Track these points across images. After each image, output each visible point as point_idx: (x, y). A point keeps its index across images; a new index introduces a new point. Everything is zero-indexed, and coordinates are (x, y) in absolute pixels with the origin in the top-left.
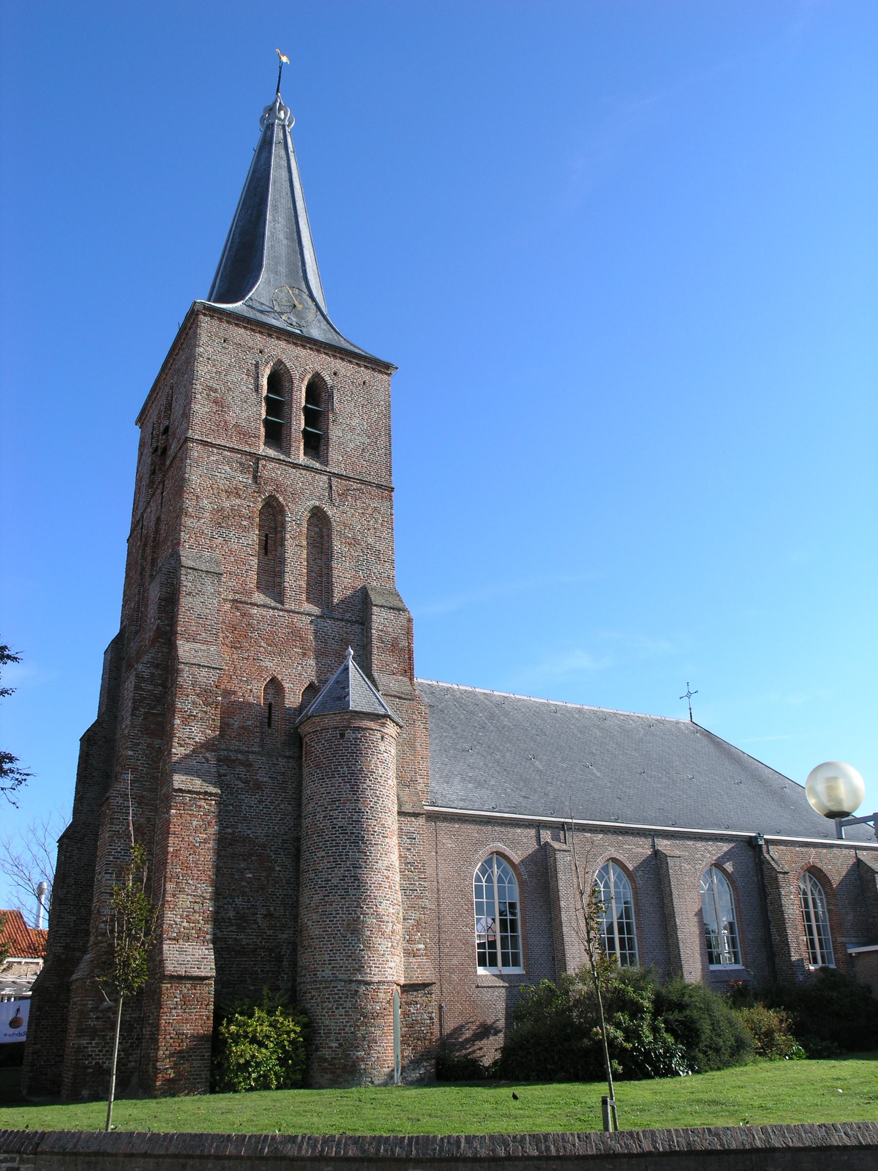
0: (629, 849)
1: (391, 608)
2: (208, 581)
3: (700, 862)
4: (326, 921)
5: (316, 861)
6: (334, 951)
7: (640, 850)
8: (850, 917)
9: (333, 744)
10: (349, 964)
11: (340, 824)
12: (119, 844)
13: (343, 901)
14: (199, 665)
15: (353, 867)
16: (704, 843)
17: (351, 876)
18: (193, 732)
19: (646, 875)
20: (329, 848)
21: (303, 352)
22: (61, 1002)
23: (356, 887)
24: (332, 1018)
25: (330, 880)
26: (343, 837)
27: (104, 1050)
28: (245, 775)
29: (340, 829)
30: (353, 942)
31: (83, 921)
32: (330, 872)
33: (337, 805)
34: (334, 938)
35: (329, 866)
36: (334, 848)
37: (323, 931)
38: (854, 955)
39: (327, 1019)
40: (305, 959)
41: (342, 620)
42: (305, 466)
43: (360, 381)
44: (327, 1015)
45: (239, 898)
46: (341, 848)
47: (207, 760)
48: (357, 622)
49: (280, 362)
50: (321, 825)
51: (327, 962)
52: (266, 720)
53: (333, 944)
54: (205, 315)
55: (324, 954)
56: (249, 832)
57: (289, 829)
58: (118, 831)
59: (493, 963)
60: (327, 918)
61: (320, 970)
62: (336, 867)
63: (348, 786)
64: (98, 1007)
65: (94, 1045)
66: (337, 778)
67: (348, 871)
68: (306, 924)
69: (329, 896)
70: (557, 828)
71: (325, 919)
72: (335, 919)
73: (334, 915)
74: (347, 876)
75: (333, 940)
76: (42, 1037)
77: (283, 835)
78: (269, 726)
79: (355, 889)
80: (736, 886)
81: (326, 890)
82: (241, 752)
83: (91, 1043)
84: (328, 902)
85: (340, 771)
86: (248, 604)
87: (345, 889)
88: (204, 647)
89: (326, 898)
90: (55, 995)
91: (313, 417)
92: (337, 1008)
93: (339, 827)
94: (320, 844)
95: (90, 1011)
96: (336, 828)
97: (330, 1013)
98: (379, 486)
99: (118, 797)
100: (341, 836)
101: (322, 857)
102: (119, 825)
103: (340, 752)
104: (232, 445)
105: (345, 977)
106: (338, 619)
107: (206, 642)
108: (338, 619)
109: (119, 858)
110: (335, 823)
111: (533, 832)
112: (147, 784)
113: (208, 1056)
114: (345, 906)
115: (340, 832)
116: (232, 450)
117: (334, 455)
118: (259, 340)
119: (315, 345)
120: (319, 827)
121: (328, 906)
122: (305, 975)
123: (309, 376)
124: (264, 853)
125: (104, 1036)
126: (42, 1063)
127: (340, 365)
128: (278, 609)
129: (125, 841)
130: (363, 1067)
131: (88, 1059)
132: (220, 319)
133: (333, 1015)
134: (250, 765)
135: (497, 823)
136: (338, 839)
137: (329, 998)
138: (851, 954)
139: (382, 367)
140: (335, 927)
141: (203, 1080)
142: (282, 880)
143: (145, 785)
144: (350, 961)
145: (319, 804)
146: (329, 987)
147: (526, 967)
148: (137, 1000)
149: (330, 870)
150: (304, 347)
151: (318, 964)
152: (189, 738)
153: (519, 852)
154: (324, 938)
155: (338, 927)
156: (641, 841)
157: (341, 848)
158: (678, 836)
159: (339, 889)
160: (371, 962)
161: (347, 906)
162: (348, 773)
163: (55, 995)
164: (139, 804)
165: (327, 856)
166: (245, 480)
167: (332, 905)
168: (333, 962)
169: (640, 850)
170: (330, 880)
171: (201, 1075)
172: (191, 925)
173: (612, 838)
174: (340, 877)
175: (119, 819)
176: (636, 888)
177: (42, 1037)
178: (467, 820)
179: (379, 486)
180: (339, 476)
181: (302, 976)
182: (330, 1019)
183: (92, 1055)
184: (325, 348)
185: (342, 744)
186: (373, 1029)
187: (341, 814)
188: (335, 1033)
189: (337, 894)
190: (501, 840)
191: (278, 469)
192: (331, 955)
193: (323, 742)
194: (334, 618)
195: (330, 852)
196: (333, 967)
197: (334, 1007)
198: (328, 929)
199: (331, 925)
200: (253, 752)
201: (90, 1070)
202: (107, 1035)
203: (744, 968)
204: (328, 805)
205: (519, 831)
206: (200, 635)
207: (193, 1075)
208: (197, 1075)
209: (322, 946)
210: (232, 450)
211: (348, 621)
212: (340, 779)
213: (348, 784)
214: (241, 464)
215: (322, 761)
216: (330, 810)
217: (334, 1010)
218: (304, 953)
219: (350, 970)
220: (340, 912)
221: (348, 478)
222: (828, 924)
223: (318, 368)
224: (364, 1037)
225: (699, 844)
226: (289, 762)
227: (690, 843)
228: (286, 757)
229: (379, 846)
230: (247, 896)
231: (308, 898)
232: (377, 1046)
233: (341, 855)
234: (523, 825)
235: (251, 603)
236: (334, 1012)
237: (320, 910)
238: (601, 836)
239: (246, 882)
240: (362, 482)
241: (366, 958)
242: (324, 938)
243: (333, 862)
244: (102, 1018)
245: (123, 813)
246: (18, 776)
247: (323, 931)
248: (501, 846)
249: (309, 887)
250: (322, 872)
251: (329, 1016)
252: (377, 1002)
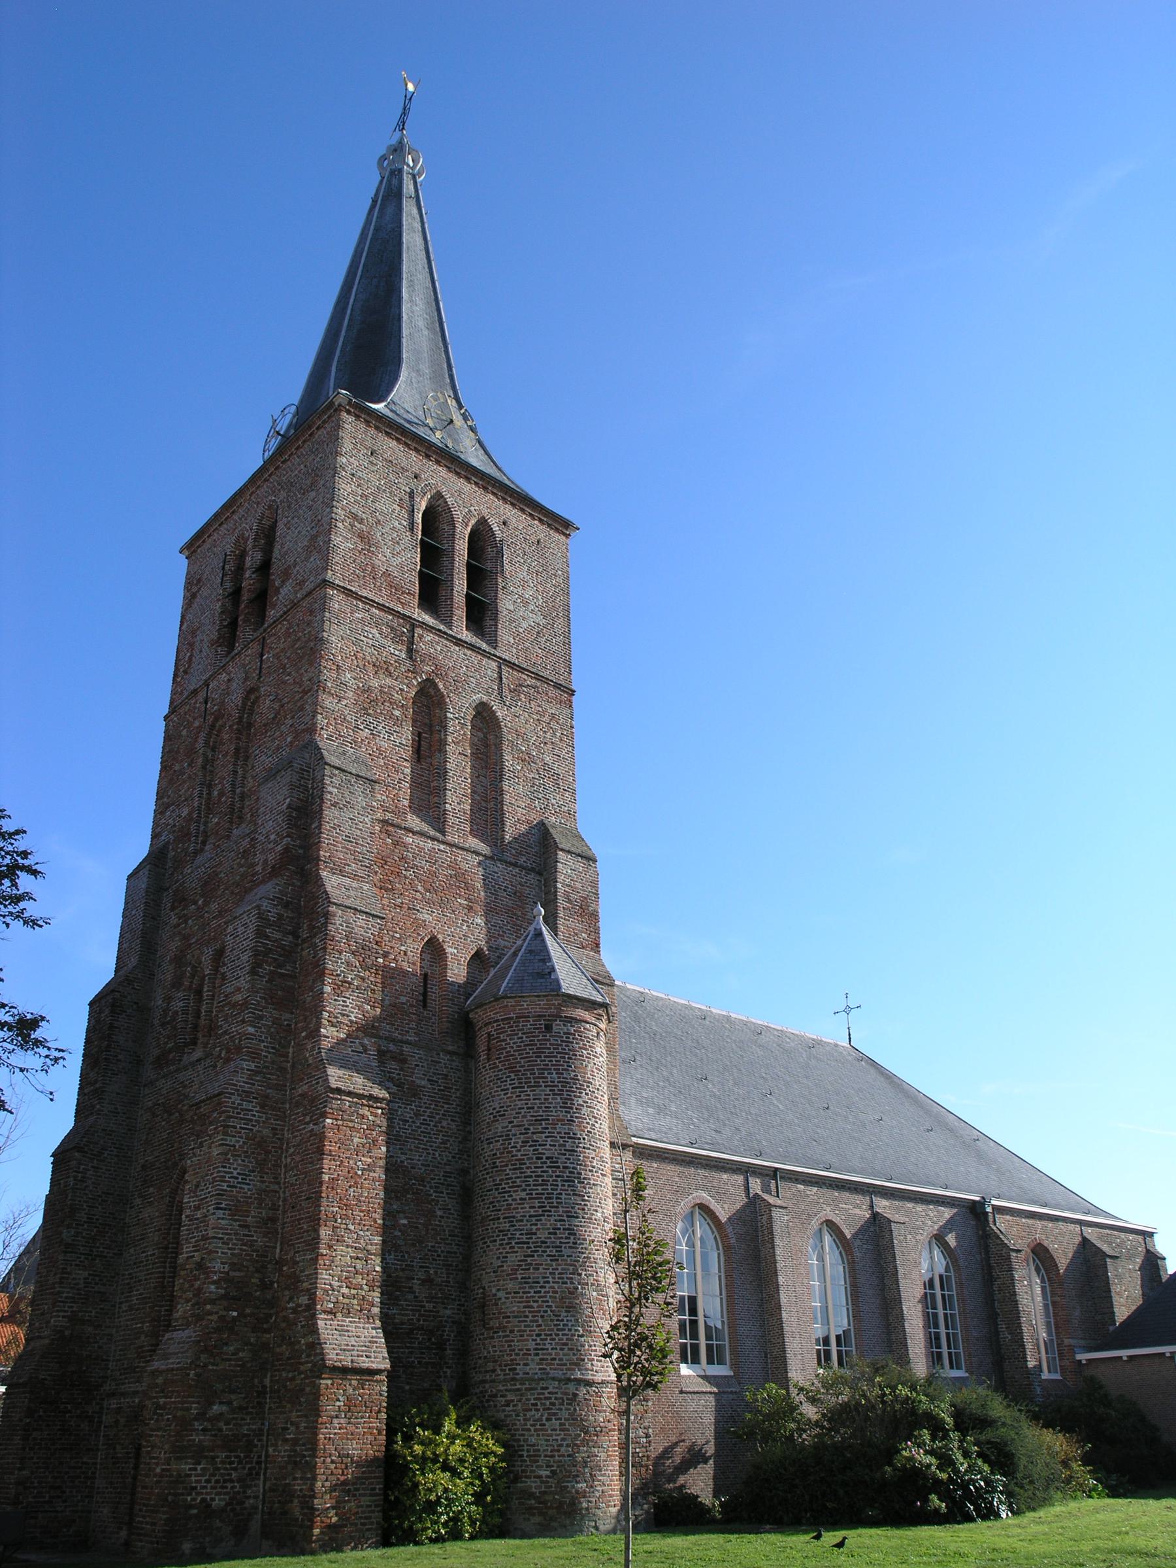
0: (846, 1210)
1: (579, 855)
2: (358, 788)
3: (921, 1231)
4: (529, 1293)
5: (511, 1205)
6: (543, 1337)
7: (857, 1211)
8: (1077, 1313)
10: (564, 1355)
11: (548, 1154)
12: (235, 1166)
13: (554, 1263)
14: (356, 909)
15: (568, 1216)
16: (924, 1207)
17: (564, 1229)
18: (347, 1006)
19: (865, 1246)
20: (532, 1187)
21: (468, 488)
22: (64, 1403)
23: (571, 1245)
24: (541, 1433)
25: (535, 1234)
26: (553, 1172)
27: (213, 1479)
28: (399, 1074)
30: (570, 1324)
31: (97, 1279)
32: (534, 1222)
33: (544, 1126)
34: (542, 1317)
35: (532, 1213)
36: (540, 1188)
37: (524, 1307)
38: (1084, 1362)
39: (533, 1435)
40: (495, 1346)
41: (515, 865)
43: (534, 539)
44: (532, 1429)
45: (390, 1255)
46: (549, 1187)
47: (366, 1050)
48: (533, 870)
49: (439, 496)
50: (519, 1154)
51: (532, 1352)
52: (421, 998)
53: (540, 1326)
54: (349, 412)
55: (528, 1340)
56: (404, 1157)
57: (454, 1157)
58: (234, 1146)
59: (696, 1360)
60: (531, 1287)
61: (521, 1363)
62: (544, 1215)
63: (559, 1100)
64: (204, 1414)
65: (199, 1471)
66: (543, 1088)
67: (560, 1221)
68: (495, 1295)
69: (533, 1256)
70: (767, 1175)
71: (527, 1290)
72: (543, 1290)
73: (542, 1284)
74: (559, 1229)
75: (540, 1320)
76: (32, 1458)
77: (445, 1164)
78: (425, 1006)
79: (570, 1247)
80: (959, 1266)
81: (528, 1248)
82: (394, 1041)
83: (195, 1469)
84: (531, 1264)
85: (547, 1078)
86: (401, 828)
87: (557, 1247)
88: (355, 884)
89: (529, 1259)
90: (53, 1392)
92: (548, 1420)
93: (547, 1158)
94: (518, 1180)
95: (196, 1419)
96: (542, 1158)
97: (538, 1427)
98: (558, 686)
99: (233, 1094)
100: (550, 1170)
101: (521, 1199)
102: (235, 1136)
104: (381, 602)
105: (559, 1374)
106: (511, 864)
107: (355, 877)
108: (511, 864)
109: (236, 1187)
110: (540, 1151)
111: (740, 1179)
112: (272, 1077)
113: (380, 1489)
114: (557, 1272)
115: (549, 1164)
116: (382, 607)
117: (505, 635)
118: (413, 460)
119: (482, 479)
120: (516, 1156)
121: (531, 1271)
122: (494, 1371)
123: (473, 522)
124: (422, 1190)
125: (213, 1458)
126: (31, 1500)
128: (438, 841)
129: (243, 1161)
130: (585, 1505)
131: (190, 1494)
132: (367, 423)
133: (542, 1430)
134: (404, 1061)
135: (701, 1164)
136: (545, 1174)
137: (536, 1404)
138: (1080, 1361)
140: (543, 1301)
141: (374, 1527)
142: (444, 1231)
143: (270, 1079)
144: (566, 1351)
145: (515, 1123)
146: (536, 1389)
147: (734, 1366)
148: (258, 1403)
149: (534, 1219)
150: (468, 479)
151: (518, 1355)
152: (343, 1015)
153: (726, 1206)
154: (527, 1317)
155: (548, 1302)
156: (859, 1199)
157: (549, 1187)
158: (897, 1196)
159: (548, 1247)
160: (593, 1353)
161: (560, 1271)
162: (558, 1082)
163: (53, 1392)
164: (262, 1107)
165: (530, 1199)
166: (397, 653)
167: (538, 1269)
168: (540, 1352)
169: (857, 1211)
170: (535, 1234)
171: (370, 1518)
172: (353, 1292)
173: (827, 1192)
174: (549, 1229)
175: (235, 1127)
176: (854, 1262)
177: (32, 1458)
178: (666, 1158)
179: (558, 686)
180: (512, 665)
181: (487, 1372)
182: (538, 1435)
183: (196, 1487)
184: (494, 486)
185: (549, 1040)
186: (596, 1450)
187: (549, 1139)
188: (546, 1456)
189: (545, 1255)
191: (438, 643)
192: (538, 1342)
193: (520, 1035)
194: (506, 862)
195: (534, 1192)
196: (541, 1359)
197: (544, 1418)
198: (532, 1303)
199: (537, 1298)
200: (408, 1043)
201: (195, 1511)
202: (218, 1457)
203: (967, 1375)
204: (530, 1125)
205: (725, 1176)
206: (349, 865)
207: (361, 1518)
208: (366, 1518)
209: (523, 1328)
210: (382, 607)
211: (522, 867)
212: (548, 1089)
213: (558, 1097)
214: (392, 629)
215: (520, 1062)
216: (533, 1133)
217: (544, 1422)
218: (493, 1338)
219: (566, 1365)
220: (550, 1279)
221: (522, 670)
223: (485, 512)
224: (586, 1462)
225: (920, 1208)
226: (453, 1061)
227: (910, 1205)
228: (449, 1052)
229: (599, 1188)
230: (402, 1252)
231: (498, 1258)
232: (601, 1475)
233: (550, 1198)
234: (730, 1169)
235: (405, 828)
236: (544, 1425)
237: (519, 1277)
238: (815, 1189)
239: (400, 1231)
240: (538, 677)
241: (587, 1347)
242: (527, 1317)
243: (539, 1207)
244: (210, 1430)
245: (241, 1119)
246: (45, 1052)
247: (524, 1307)
249: (498, 1242)
250: (522, 1221)
251: (536, 1430)
252: (600, 1412)
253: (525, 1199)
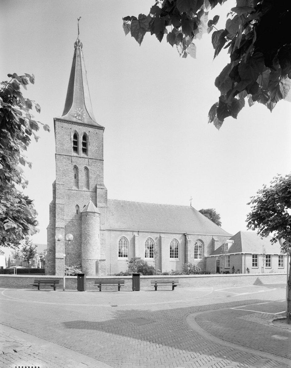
2: (61, 186)
21: (81, 127)
49: (76, 131)
54: (57, 121)
88: (61, 200)
98: (100, 160)
107: (62, 199)
111: (132, 233)
116: (66, 155)
117: (89, 153)
118: (70, 126)
127: (91, 129)
139: (102, 128)
173: (149, 233)
179: (100, 160)
210: (66, 155)
221: (93, 159)
240: (96, 159)
248: (124, 236)
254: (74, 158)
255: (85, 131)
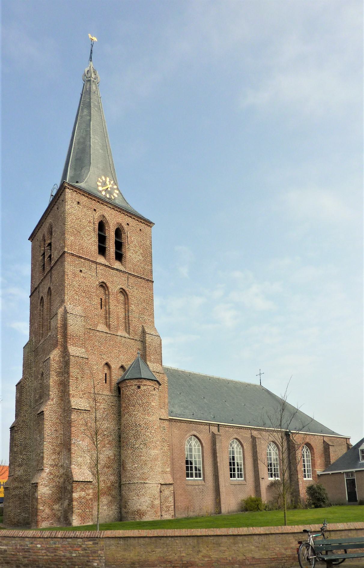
9: (135, 391)
10: (143, 476)
21: (114, 212)
29: (139, 425)
30: (145, 468)
36: (136, 433)
38: (319, 475)
42: (116, 269)
49: (104, 216)
66: (137, 405)
91: (119, 245)
101: (131, 436)
103: (138, 394)
115: (139, 426)
190: (195, 430)
195: (135, 434)
213: (142, 407)
217: (138, 493)
222: (311, 464)
253: (132, 436)
254: (102, 267)
255: (120, 220)
